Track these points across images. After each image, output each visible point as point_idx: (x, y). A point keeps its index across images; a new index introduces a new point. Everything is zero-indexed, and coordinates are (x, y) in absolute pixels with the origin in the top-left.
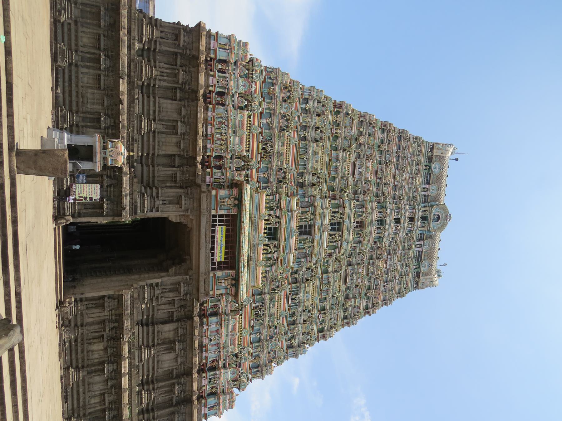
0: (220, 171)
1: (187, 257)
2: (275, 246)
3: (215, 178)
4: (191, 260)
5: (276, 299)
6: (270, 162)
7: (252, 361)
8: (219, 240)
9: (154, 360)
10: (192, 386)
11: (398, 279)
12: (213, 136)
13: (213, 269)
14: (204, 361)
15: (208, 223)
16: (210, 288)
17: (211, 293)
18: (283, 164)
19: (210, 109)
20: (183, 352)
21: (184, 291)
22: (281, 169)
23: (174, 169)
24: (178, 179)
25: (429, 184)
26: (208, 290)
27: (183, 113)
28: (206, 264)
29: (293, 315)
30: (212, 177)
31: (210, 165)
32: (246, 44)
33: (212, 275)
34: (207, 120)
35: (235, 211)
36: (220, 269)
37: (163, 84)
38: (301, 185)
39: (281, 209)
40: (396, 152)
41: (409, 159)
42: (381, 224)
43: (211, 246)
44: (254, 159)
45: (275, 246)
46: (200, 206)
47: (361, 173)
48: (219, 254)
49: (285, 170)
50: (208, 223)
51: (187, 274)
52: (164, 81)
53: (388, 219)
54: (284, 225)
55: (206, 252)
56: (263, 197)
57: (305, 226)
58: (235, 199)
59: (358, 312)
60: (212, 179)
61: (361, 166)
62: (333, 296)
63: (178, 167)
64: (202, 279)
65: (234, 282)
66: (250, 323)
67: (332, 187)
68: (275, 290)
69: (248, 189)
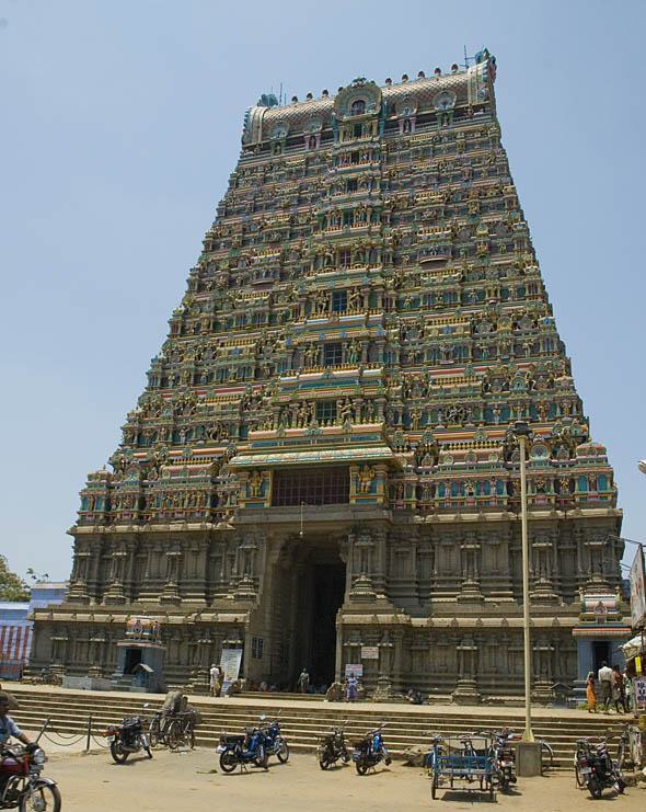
1: (330, 537)
7: (543, 418)
9: (486, 581)
10: (542, 520)
20: (482, 537)
27: (158, 549)
29: (477, 352)
32: (90, 477)
37: (129, 575)
42: (352, 215)
44: (224, 449)
52: (126, 573)
59: (505, 223)
65: (366, 467)
66: (470, 429)
67: (283, 316)
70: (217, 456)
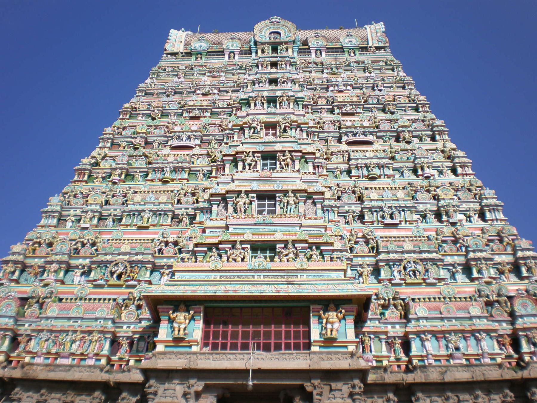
1: (282, 396)
11: (370, 73)
12: (73, 354)
13: (308, 346)
14: (499, 360)
15: (215, 356)
19: (32, 361)
25: (223, 52)
34: (47, 365)
36: (308, 335)
38: (193, 218)
39: (220, 243)
40: (168, 96)
41: (182, 79)
42: (275, 102)
47: (189, 138)
53: (266, 94)
54: (248, 236)
57: (259, 206)
61: (179, 138)
62: (393, 158)
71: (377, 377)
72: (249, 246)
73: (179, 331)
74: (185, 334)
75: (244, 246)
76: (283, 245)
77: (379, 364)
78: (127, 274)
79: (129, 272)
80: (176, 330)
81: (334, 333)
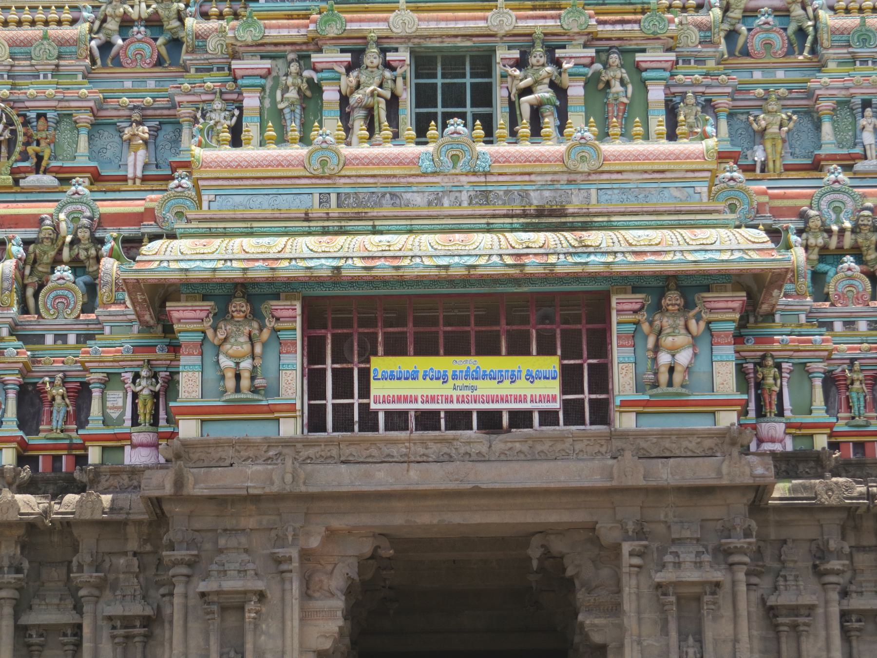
0: (96, 394)
1: (535, 553)
2: (521, 63)
3: (135, 422)
4: (544, 531)
5: (852, 21)
6: (65, 116)
8: (446, 390)
13: (601, 413)
16: (701, 424)
17: (728, 419)
18: (76, 42)
21: (698, 565)
22: (106, 47)
23: (87, 631)
24: (137, 609)
26: (710, 435)
28: (565, 456)
30: (128, 437)
31: (71, 447)
33: (626, 421)
35: (291, 312)
36: (601, 378)
39: (316, 43)
43: (473, 433)
44: (44, 210)
45: (521, 63)
46: (255, 499)
48: (522, 387)
49: (112, 25)
50: (346, 451)
51: (616, 548)
55: (504, 458)
56: (219, 164)
58: (222, 315)
60: (137, 438)
63: (78, 608)
64: (635, 474)
65: (673, 299)
68: (801, 32)
69: (164, 257)
70: (19, 235)
71: (793, 489)
72: (404, 55)
73: (238, 377)
74: (255, 390)
75: (390, 56)
76: (516, 54)
77: (803, 445)
78: (19, 148)
79: (21, 139)
80: (230, 375)
81: (678, 377)
